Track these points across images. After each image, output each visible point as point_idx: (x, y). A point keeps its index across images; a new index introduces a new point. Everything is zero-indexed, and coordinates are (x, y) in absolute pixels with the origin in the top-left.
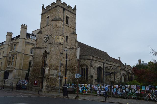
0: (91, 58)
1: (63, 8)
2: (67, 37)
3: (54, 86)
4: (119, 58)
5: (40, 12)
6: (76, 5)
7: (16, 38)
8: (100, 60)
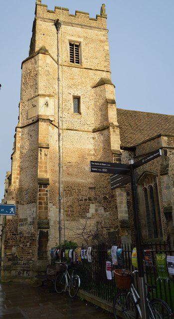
2: (77, 99)
3: (29, 257)
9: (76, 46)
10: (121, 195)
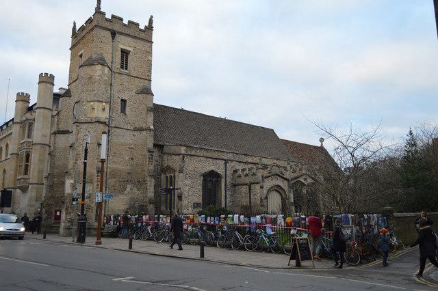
0: (183, 150)
1: (109, 30)
2: (124, 101)
4: (322, 140)
5: (69, 42)
6: (152, 17)
8: (215, 155)
9: (127, 53)
10: (150, 181)
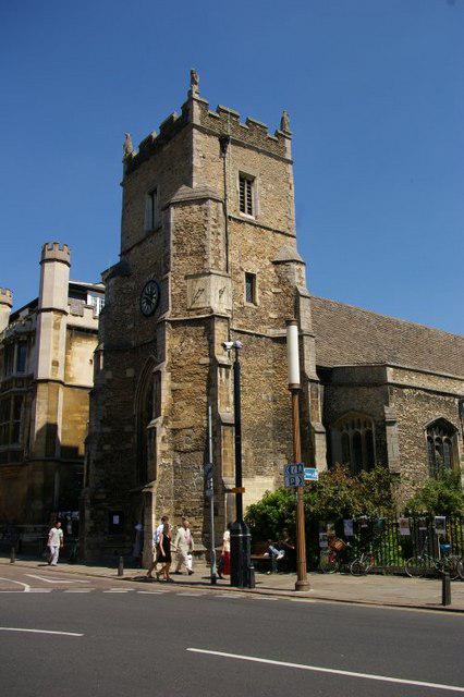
2: (250, 278)
7: (26, 312)
